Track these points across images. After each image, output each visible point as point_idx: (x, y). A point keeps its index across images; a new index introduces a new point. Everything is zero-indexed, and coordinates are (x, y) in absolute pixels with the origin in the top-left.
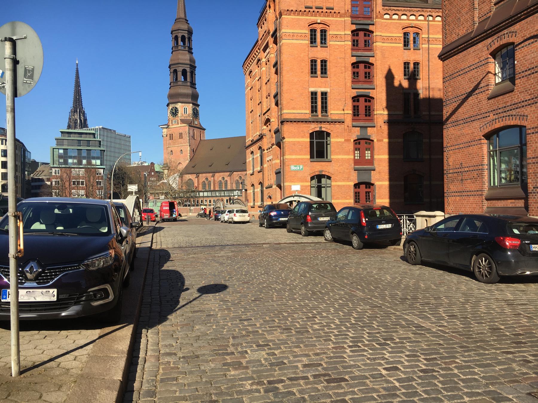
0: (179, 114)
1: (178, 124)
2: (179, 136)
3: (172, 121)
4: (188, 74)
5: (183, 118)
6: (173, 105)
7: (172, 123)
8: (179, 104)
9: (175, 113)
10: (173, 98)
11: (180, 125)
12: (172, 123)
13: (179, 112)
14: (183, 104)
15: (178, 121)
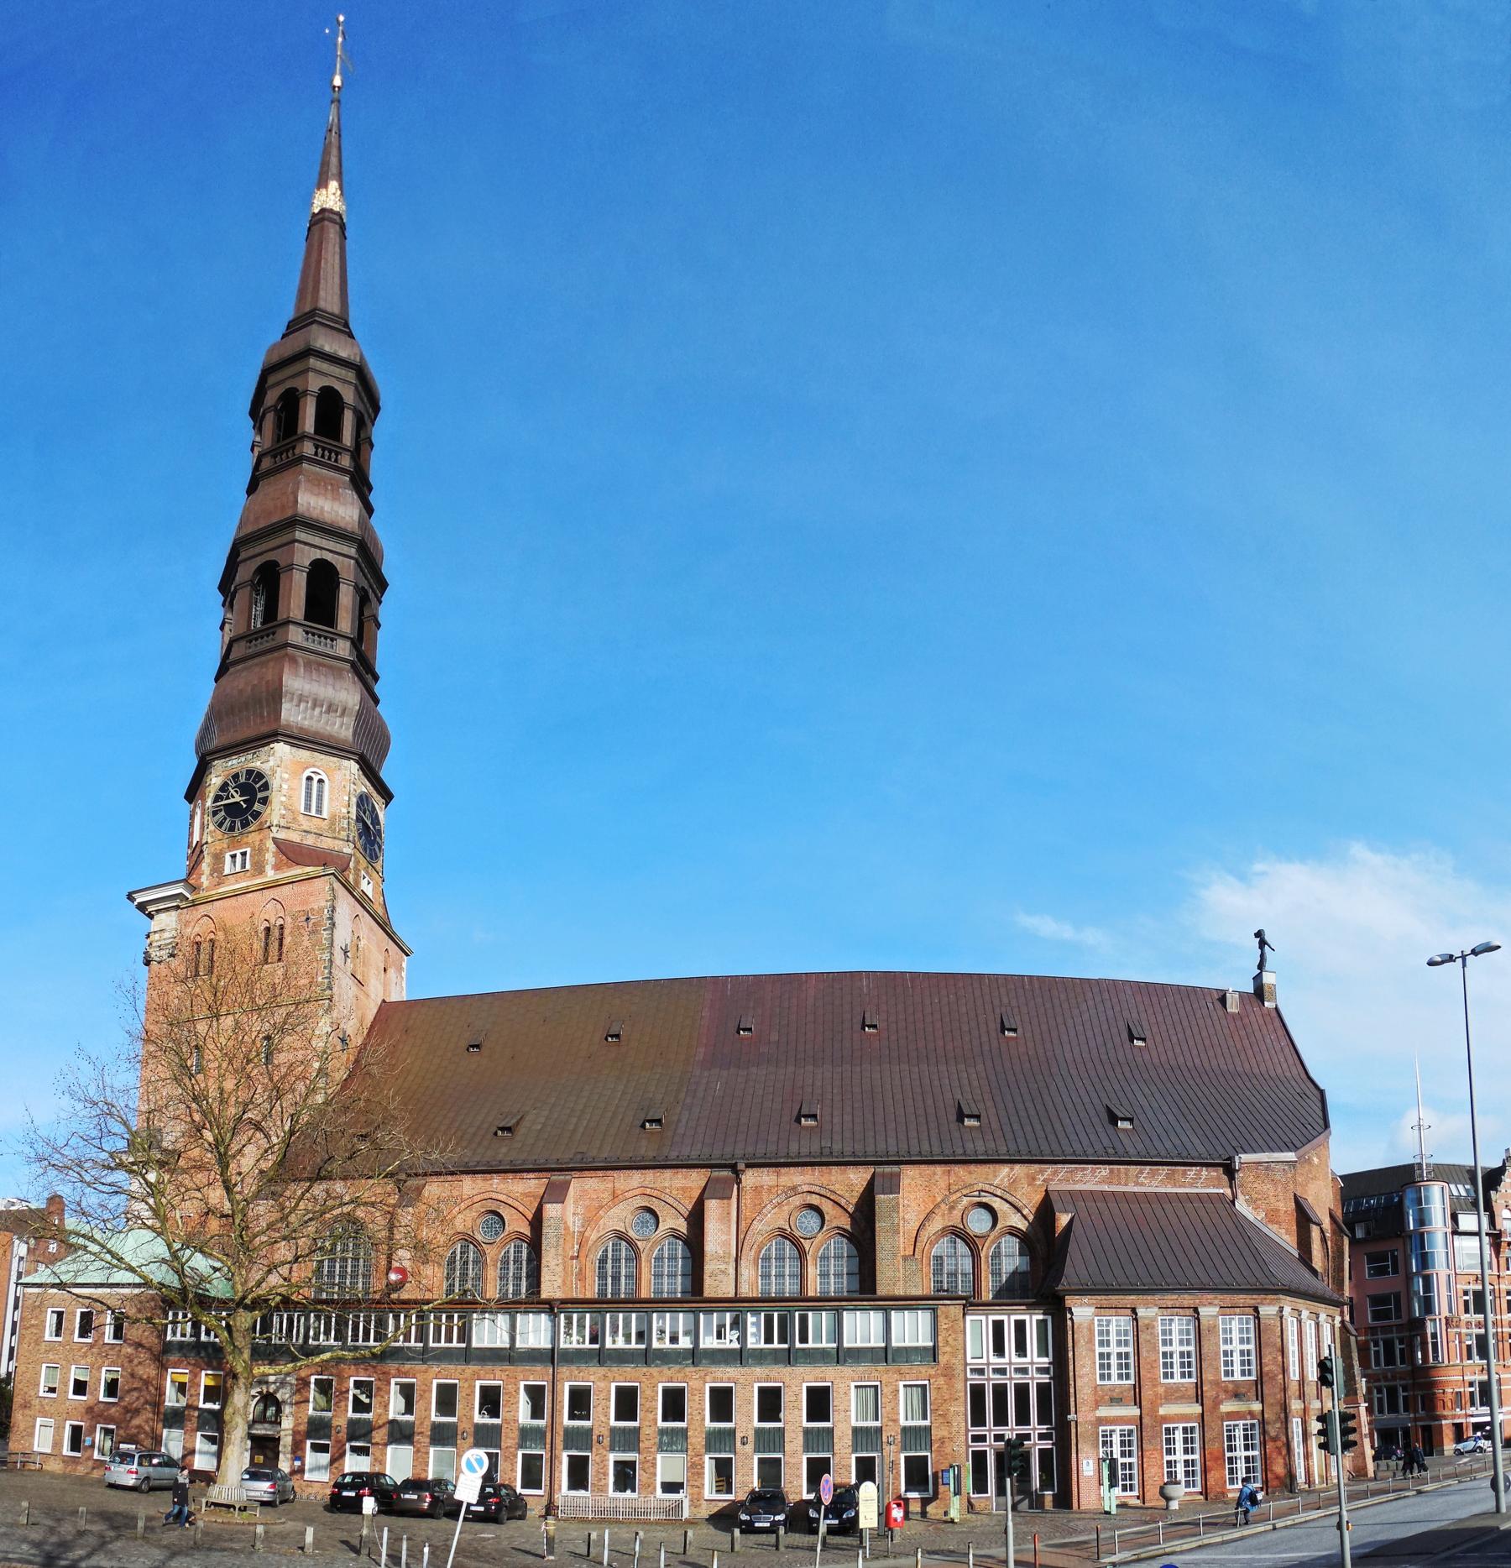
0: (275, 813)
1: (259, 869)
2: (258, 946)
3: (218, 858)
4: (346, 598)
5: (294, 837)
6: (236, 764)
7: (217, 868)
8: (281, 749)
9: (244, 805)
10: (241, 722)
11: (270, 874)
12: (217, 868)
13: (277, 798)
14: (304, 755)
15: (260, 851)
